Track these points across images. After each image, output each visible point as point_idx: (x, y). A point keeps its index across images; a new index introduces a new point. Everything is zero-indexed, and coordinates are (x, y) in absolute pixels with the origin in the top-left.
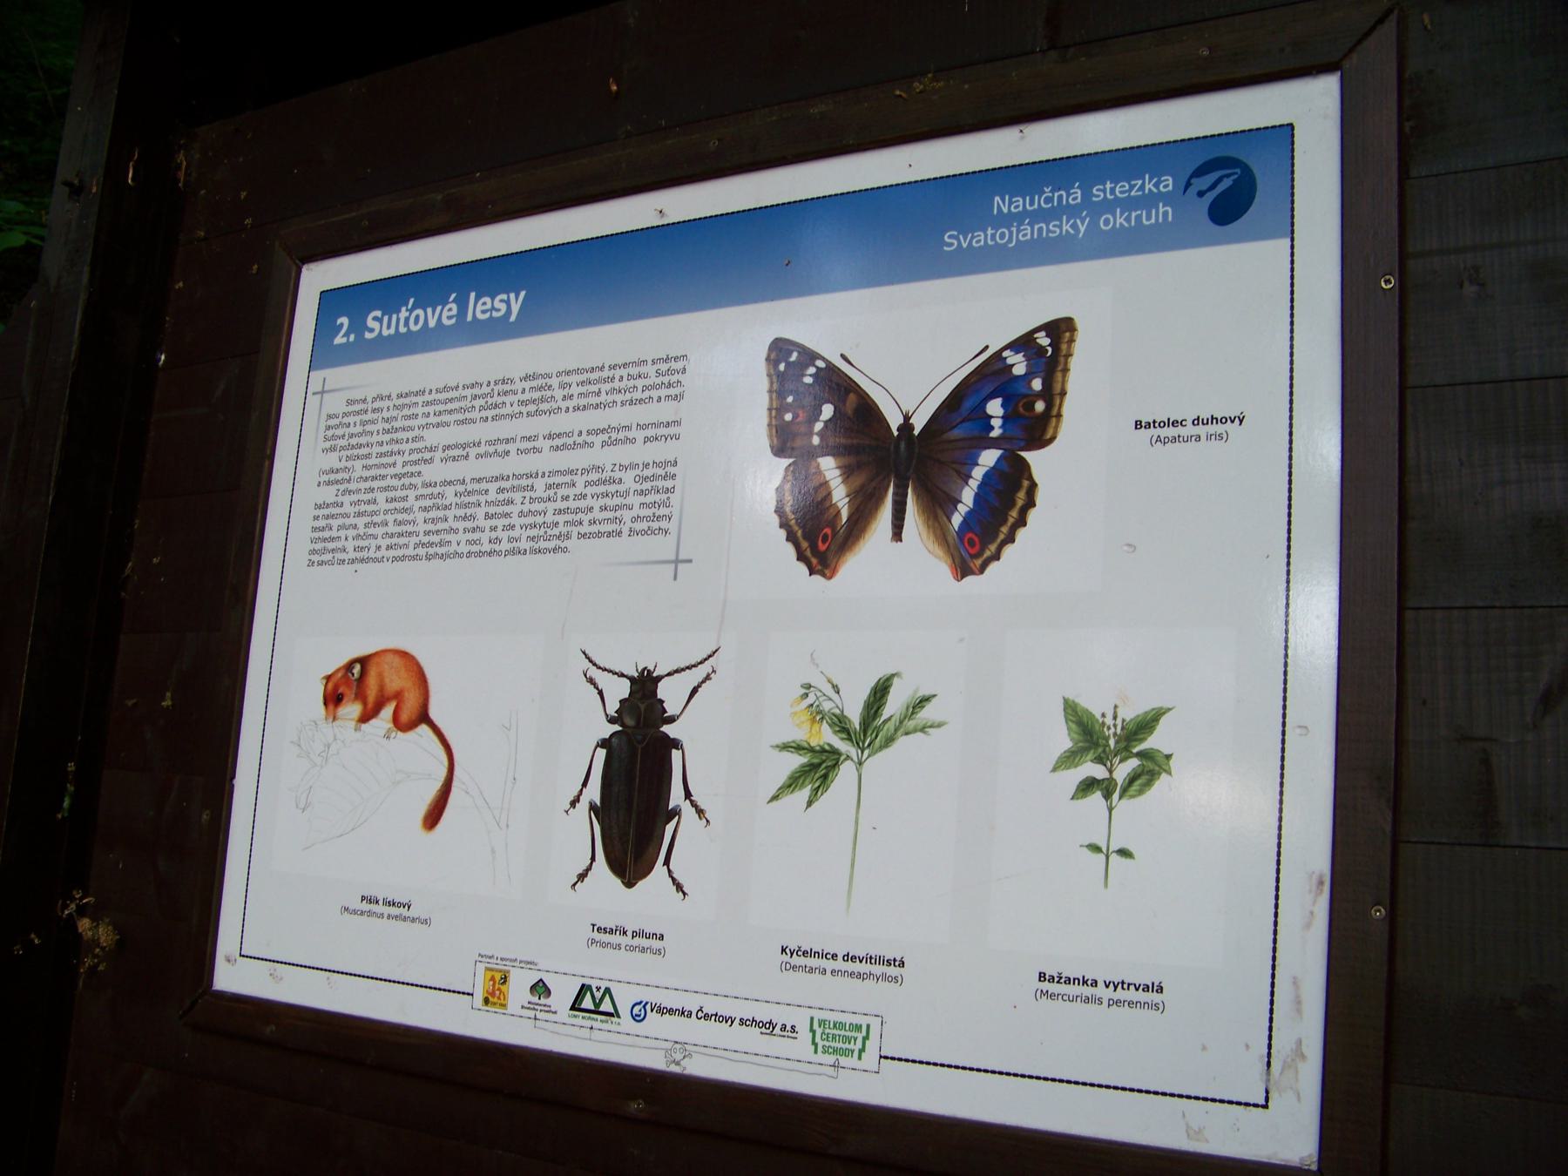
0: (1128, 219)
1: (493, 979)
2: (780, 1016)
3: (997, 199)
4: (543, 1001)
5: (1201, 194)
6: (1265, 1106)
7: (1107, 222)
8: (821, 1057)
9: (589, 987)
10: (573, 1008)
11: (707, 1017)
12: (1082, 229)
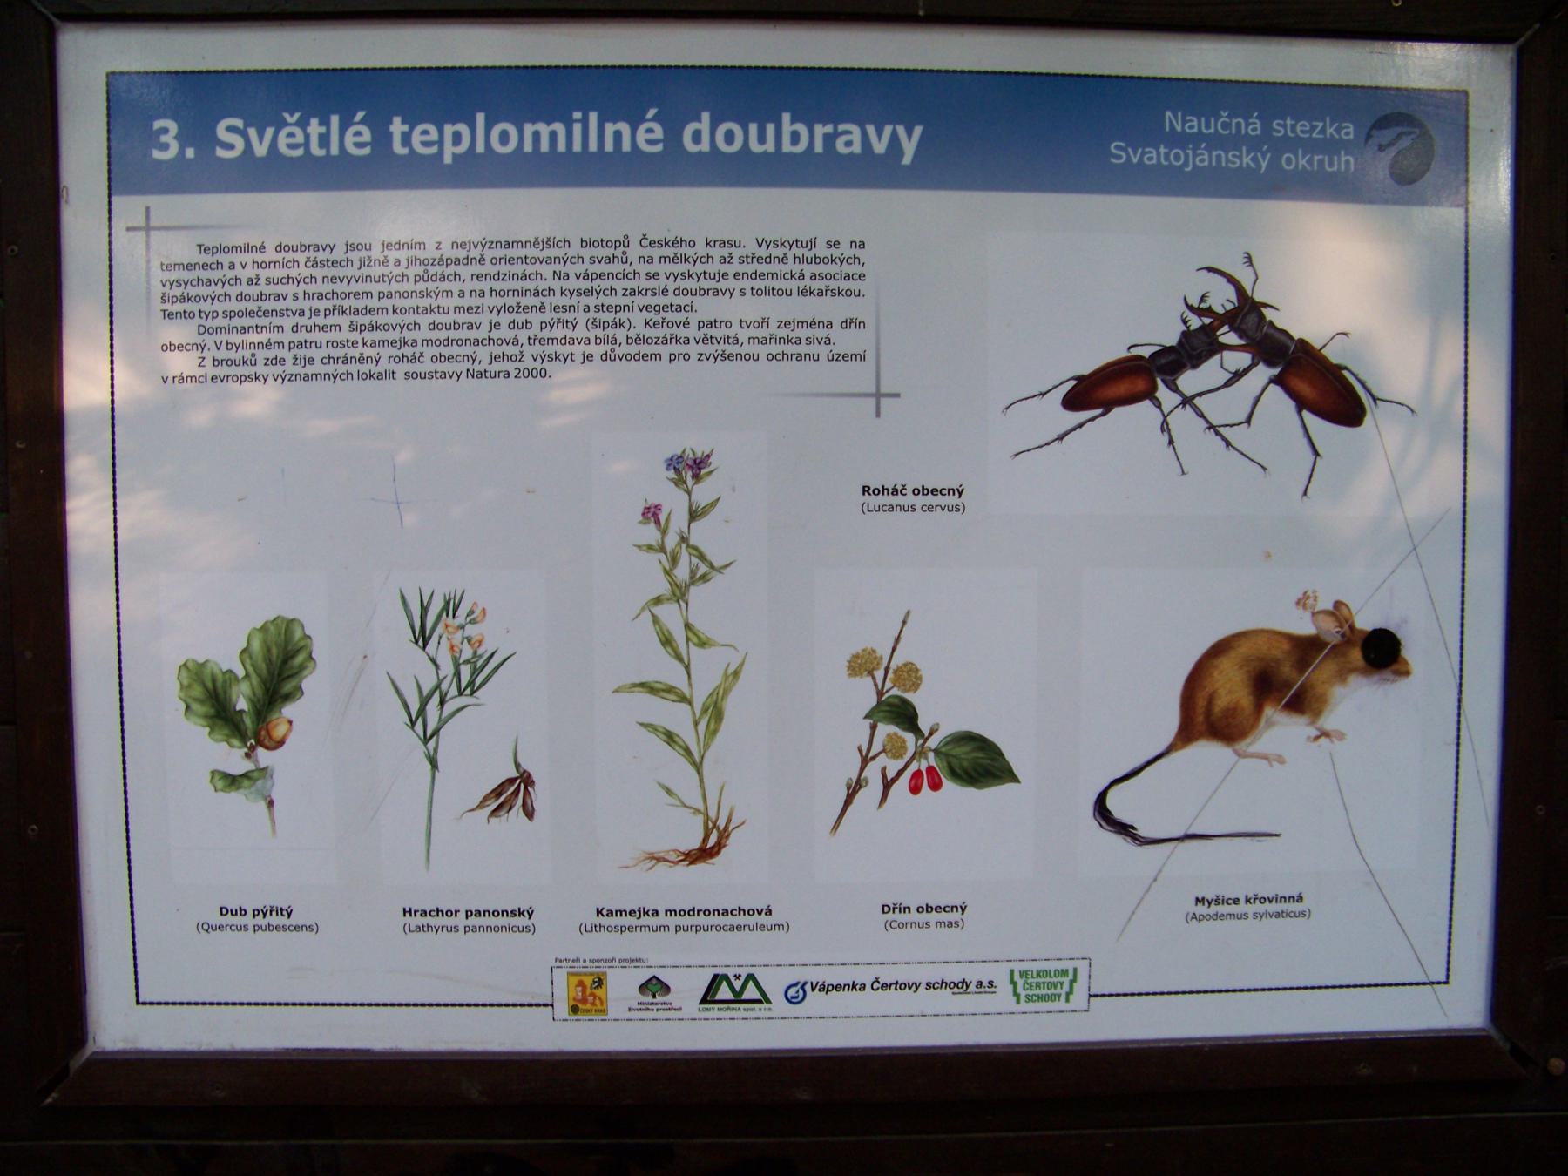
0: (1310, 162)
1: (581, 984)
2: (972, 974)
3: (1168, 114)
4: (659, 999)
5: (1381, 148)
6: (1446, 983)
7: (1289, 161)
8: (1024, 1006)
9: (726, 977)
10: (704, 1001)
11: (885, 987)
12: (1264, 165)
